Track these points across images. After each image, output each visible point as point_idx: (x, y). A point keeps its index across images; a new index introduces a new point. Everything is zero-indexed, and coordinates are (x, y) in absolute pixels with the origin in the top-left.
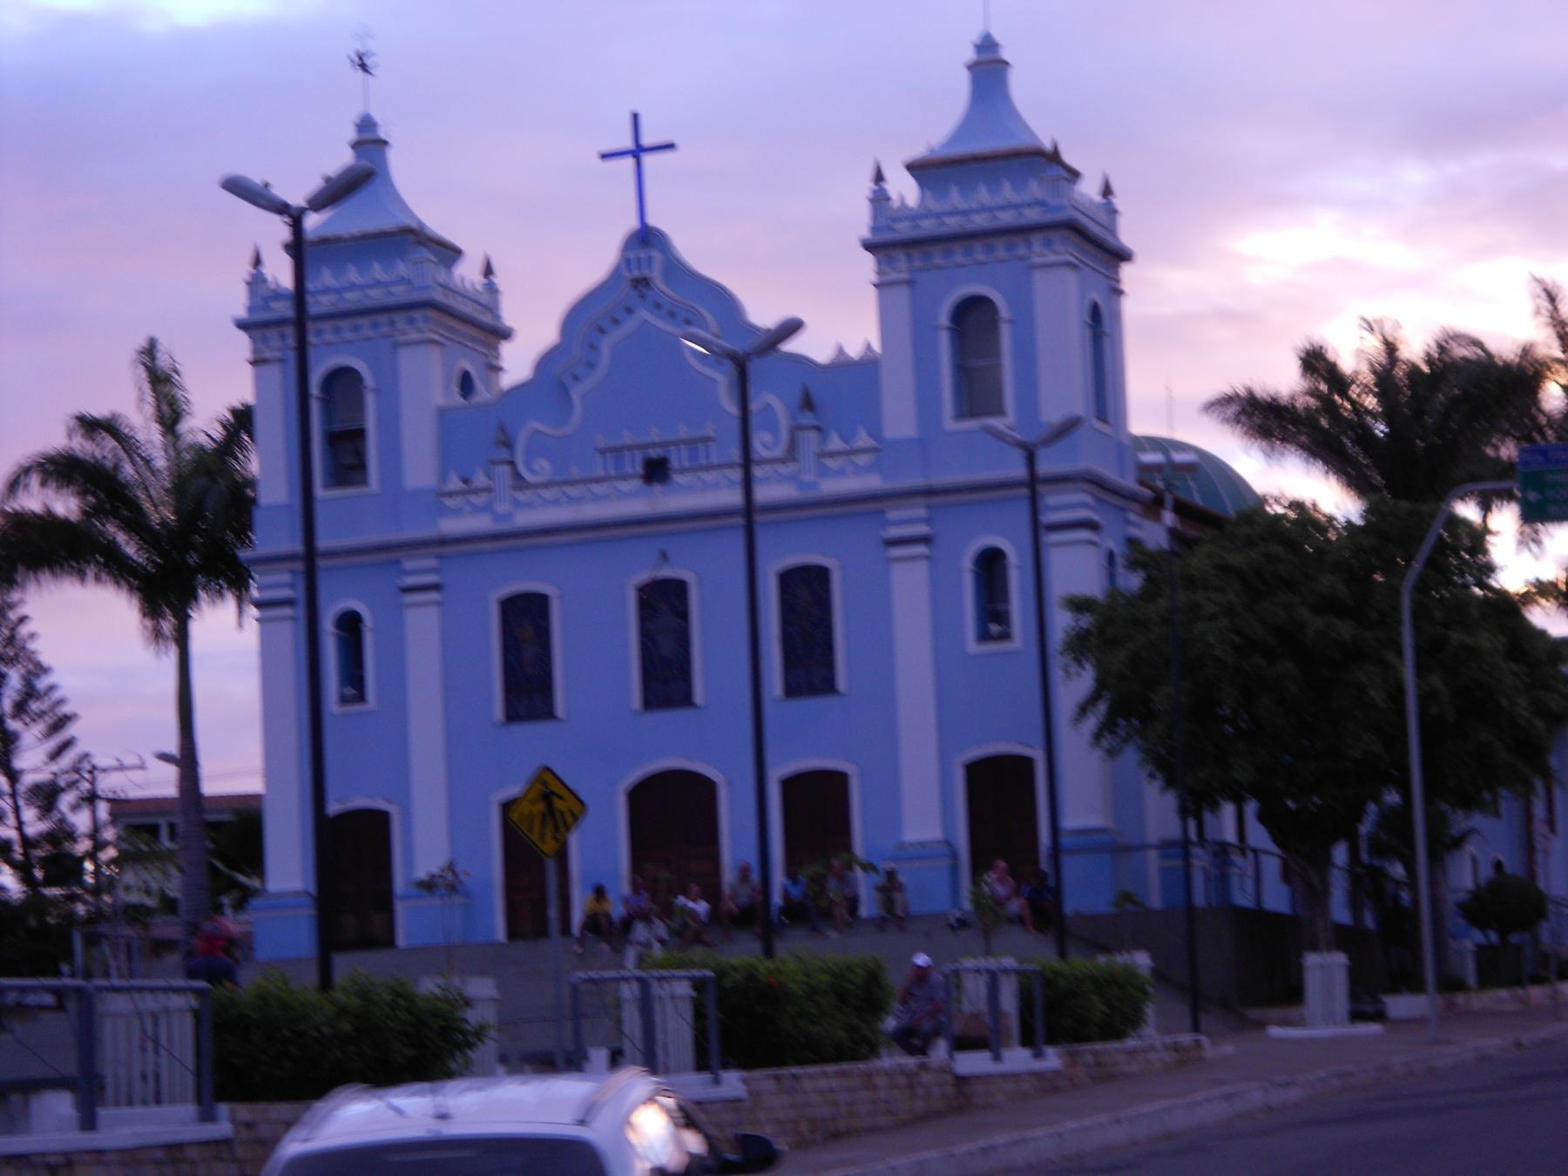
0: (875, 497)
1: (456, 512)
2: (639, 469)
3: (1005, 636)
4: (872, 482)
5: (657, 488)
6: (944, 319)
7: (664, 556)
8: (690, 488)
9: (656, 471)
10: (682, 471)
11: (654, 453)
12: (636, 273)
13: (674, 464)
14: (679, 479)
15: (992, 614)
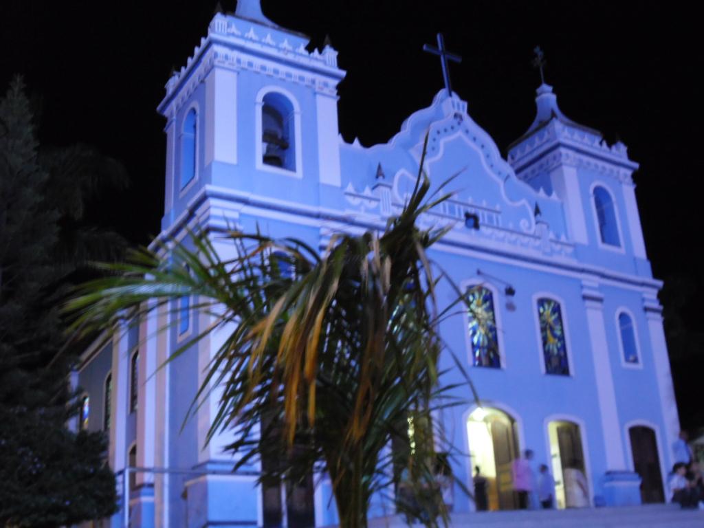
0: (582, 271)
1: (357, 208)
2: (463, 217)
3: (635, 361)
4: (574, 263)
5: (473, 231)
6: (591, 191)
7: (479, 273)
8: (489, 237)
9: (473, 221)
10: (484, 225)
11: (472, 211)
12: (456, 110)
13: (481, 221)
14: (483, 229)
15: (630, 351)
